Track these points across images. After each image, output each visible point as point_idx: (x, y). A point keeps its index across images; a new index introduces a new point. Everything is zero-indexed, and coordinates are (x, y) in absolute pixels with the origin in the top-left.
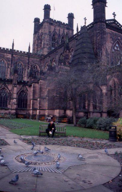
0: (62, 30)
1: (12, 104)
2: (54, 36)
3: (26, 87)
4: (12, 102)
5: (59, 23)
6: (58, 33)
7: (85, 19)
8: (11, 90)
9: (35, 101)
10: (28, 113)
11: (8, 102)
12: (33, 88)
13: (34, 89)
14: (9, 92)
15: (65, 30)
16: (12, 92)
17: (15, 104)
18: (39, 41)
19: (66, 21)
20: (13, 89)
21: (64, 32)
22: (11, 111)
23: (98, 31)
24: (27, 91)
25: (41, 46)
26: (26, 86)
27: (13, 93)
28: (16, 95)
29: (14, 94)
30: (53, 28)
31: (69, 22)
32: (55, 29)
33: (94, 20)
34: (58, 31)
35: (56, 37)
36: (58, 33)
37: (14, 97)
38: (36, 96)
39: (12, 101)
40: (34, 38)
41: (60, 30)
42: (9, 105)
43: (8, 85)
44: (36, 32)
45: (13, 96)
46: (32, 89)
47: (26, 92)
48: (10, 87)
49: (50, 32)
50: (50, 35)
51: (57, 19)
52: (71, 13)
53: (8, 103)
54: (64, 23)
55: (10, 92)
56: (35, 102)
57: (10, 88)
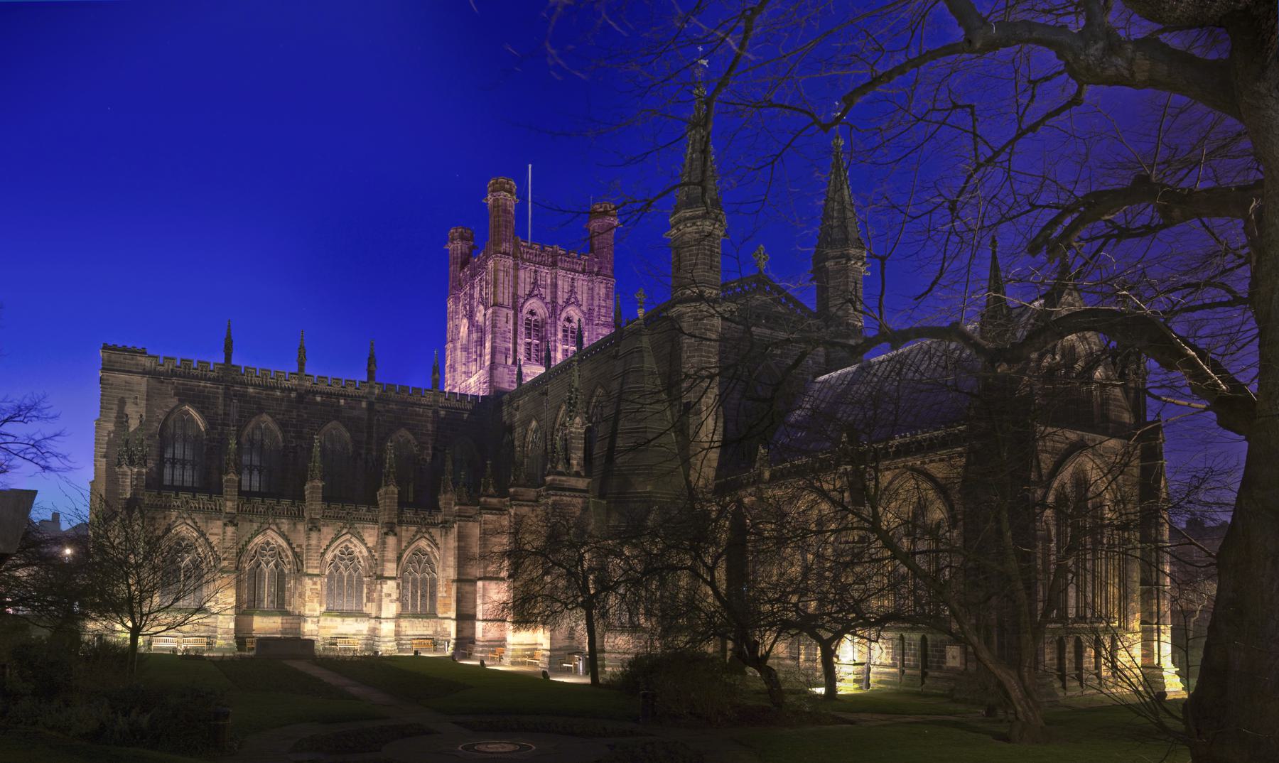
1: (381, 600)
3: (430, 533)
4: (381, 591)
8: (374, 547)
9: (467, 588)
10: (439, 629)
11: (365, 591)
12: (459, 541)
13: (462, 544)
14: (365, 553)
15: (578, 284)
16: (377, 555)
17: (391, 601)
18: (475, 336)
20: (384, 543)
22: (378, 626)
24: (435, 550)
25: (481, 356)
26: (431, 530)
27: (384, 561)
28: (395, 566)
29: (389, 561)
34: (548, 291)
36: (548, 299)
37: (386, 574)
38: (469, 570)
39: (379, 587)
41: (555, 286)
42: (369, 604)
43: (363, 528)
45: (383, 570)
46: (456, 544)
47: (433, 553)
48: (370, 536)
53: (364, 595)
55: (370, 552)
56: (467, 593)
57: (371, 539)
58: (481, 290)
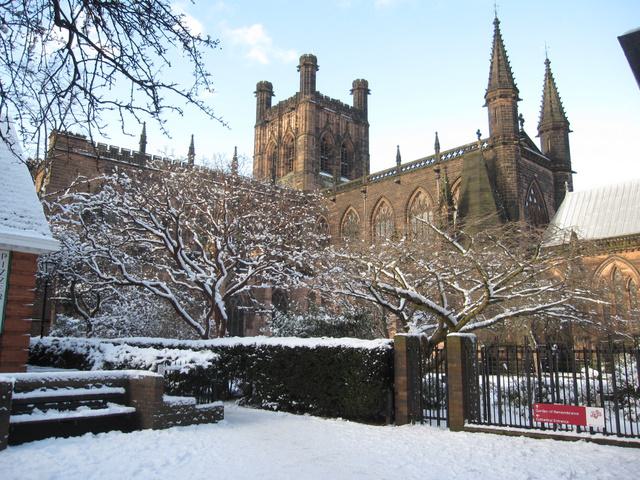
0: (343, 125)
2: (324, 139)
5: (336, 105)
6: (334, 132)
7: (479, 134)
15: (350, 125)
19: (348, 100)
21: (347, 129)
23: (507, 164)
30: (323, 117)
31: (355, 103)
32: (328, 122)
33: (493, 137)
35: (331, 141)
36: (334, 132)
40: (258, 138)
44: (263, 122)
49: (317, 129)
50: (318, 139)
51: (333, 95)
52: (363, 80)
54: (347, 106)
58: (289, 123)
